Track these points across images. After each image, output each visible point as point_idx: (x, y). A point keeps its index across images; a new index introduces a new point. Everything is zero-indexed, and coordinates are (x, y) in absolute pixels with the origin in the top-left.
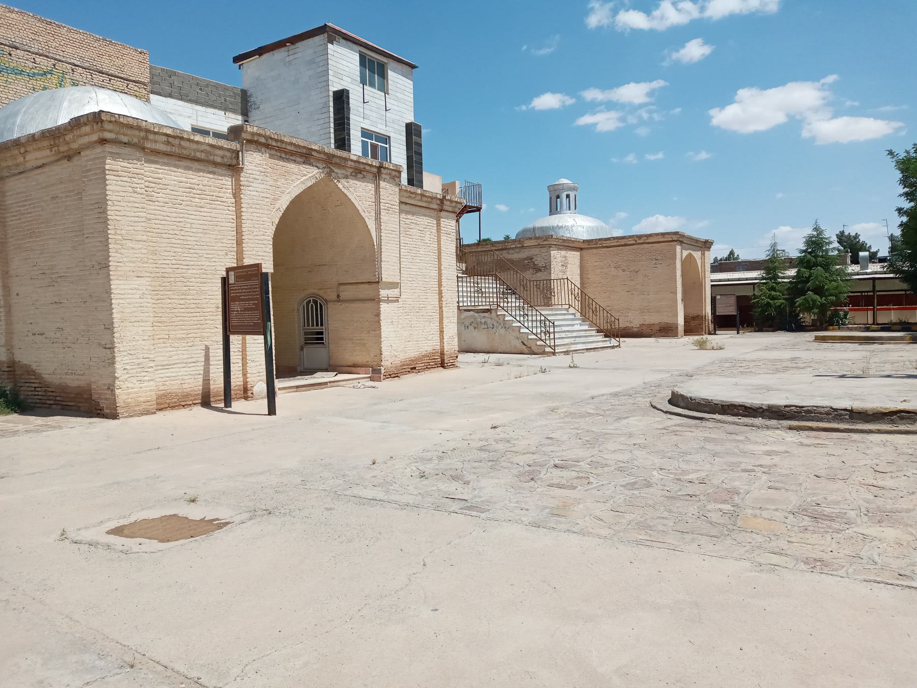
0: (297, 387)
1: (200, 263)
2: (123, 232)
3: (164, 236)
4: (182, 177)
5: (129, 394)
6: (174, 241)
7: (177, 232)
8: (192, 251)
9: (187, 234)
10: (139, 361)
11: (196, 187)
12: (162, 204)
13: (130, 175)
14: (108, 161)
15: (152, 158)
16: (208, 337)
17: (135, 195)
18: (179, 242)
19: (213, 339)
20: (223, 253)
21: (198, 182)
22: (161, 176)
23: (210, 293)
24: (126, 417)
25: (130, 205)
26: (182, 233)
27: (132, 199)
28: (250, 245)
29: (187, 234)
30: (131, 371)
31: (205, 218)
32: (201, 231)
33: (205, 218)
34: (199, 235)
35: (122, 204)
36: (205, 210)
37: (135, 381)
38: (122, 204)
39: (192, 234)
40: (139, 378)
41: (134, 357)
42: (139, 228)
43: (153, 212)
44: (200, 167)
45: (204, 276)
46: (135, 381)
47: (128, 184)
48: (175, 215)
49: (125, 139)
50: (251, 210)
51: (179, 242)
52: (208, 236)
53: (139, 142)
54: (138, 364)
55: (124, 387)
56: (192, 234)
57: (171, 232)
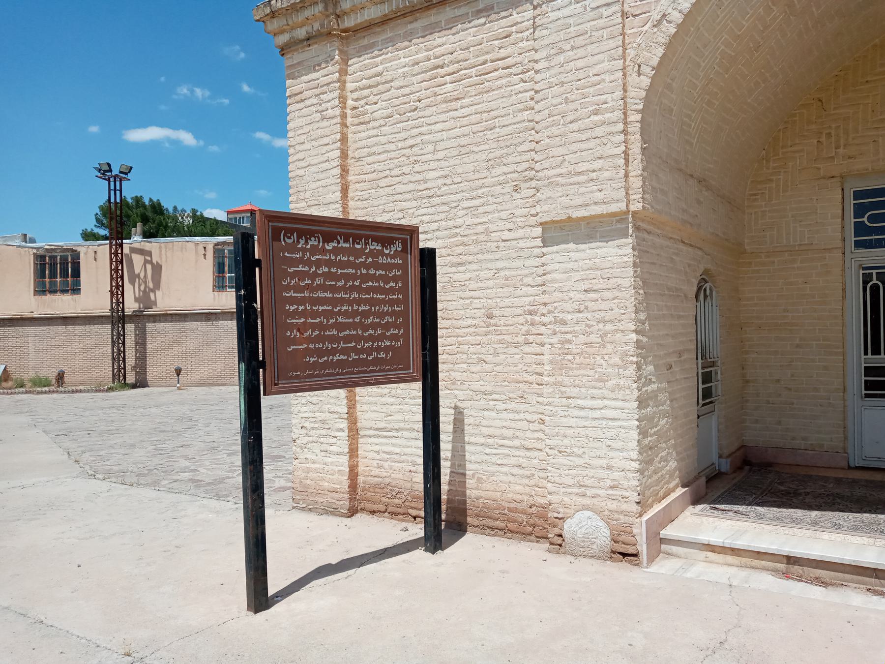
0: (790, 560)
1: (451, 223)
2: (308, 194)
3: (382, 183)
4: (417, 53)
5: (308, 470)
6: (400, 188)
7: (406, 170)
8: (437, 200)
9: (426, 167)
10: (323, 416)
11: (448, 58)
12: (382, 122)
13: (317, 91)
14: (288, 81)
15: (365, 42)
16: (463, 382)
17: (325, 123)
18: (411, 187)
19: (476, 386)
20: (508, 188)
21: (448, 47)
22: (380, 68)
23: (473, 285)
24: (303, 509)
25: (316, 143)
26: (417, 168)
27: (320, 132)
28: (556, 151)
29: (426, 167)
30: (312, 433)
31: (465, 121)
32: (455, 152)
33: (465, 121)
34: (452, 162)
35: (307, 146)
36: (467, 101)
37: (318, 451)
38: (307, 146)
39: (435, 165)
40: (324, 447)
41: (316, 408)
42: (329, 181)
43: (364, 143)
44: (458, 12)
45: (459, 250)
46: (318, 451)
47: (313, 109)
48: (403, 135)
49: (301, 33)
50: (561, 58)
51: (411, 187)
52: (472, 157)
53: (322, 26)
54: (323, 422)
55: (302, 457)
56: (435, 165)
57: (397, 172)
